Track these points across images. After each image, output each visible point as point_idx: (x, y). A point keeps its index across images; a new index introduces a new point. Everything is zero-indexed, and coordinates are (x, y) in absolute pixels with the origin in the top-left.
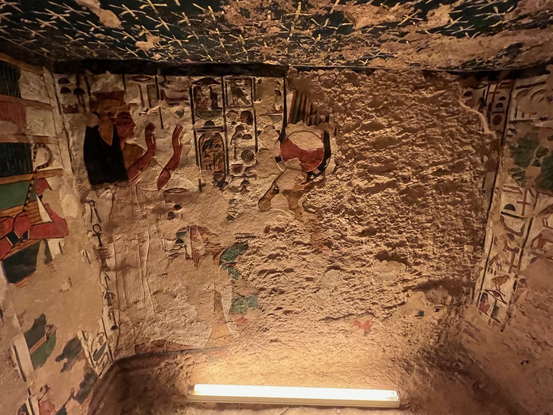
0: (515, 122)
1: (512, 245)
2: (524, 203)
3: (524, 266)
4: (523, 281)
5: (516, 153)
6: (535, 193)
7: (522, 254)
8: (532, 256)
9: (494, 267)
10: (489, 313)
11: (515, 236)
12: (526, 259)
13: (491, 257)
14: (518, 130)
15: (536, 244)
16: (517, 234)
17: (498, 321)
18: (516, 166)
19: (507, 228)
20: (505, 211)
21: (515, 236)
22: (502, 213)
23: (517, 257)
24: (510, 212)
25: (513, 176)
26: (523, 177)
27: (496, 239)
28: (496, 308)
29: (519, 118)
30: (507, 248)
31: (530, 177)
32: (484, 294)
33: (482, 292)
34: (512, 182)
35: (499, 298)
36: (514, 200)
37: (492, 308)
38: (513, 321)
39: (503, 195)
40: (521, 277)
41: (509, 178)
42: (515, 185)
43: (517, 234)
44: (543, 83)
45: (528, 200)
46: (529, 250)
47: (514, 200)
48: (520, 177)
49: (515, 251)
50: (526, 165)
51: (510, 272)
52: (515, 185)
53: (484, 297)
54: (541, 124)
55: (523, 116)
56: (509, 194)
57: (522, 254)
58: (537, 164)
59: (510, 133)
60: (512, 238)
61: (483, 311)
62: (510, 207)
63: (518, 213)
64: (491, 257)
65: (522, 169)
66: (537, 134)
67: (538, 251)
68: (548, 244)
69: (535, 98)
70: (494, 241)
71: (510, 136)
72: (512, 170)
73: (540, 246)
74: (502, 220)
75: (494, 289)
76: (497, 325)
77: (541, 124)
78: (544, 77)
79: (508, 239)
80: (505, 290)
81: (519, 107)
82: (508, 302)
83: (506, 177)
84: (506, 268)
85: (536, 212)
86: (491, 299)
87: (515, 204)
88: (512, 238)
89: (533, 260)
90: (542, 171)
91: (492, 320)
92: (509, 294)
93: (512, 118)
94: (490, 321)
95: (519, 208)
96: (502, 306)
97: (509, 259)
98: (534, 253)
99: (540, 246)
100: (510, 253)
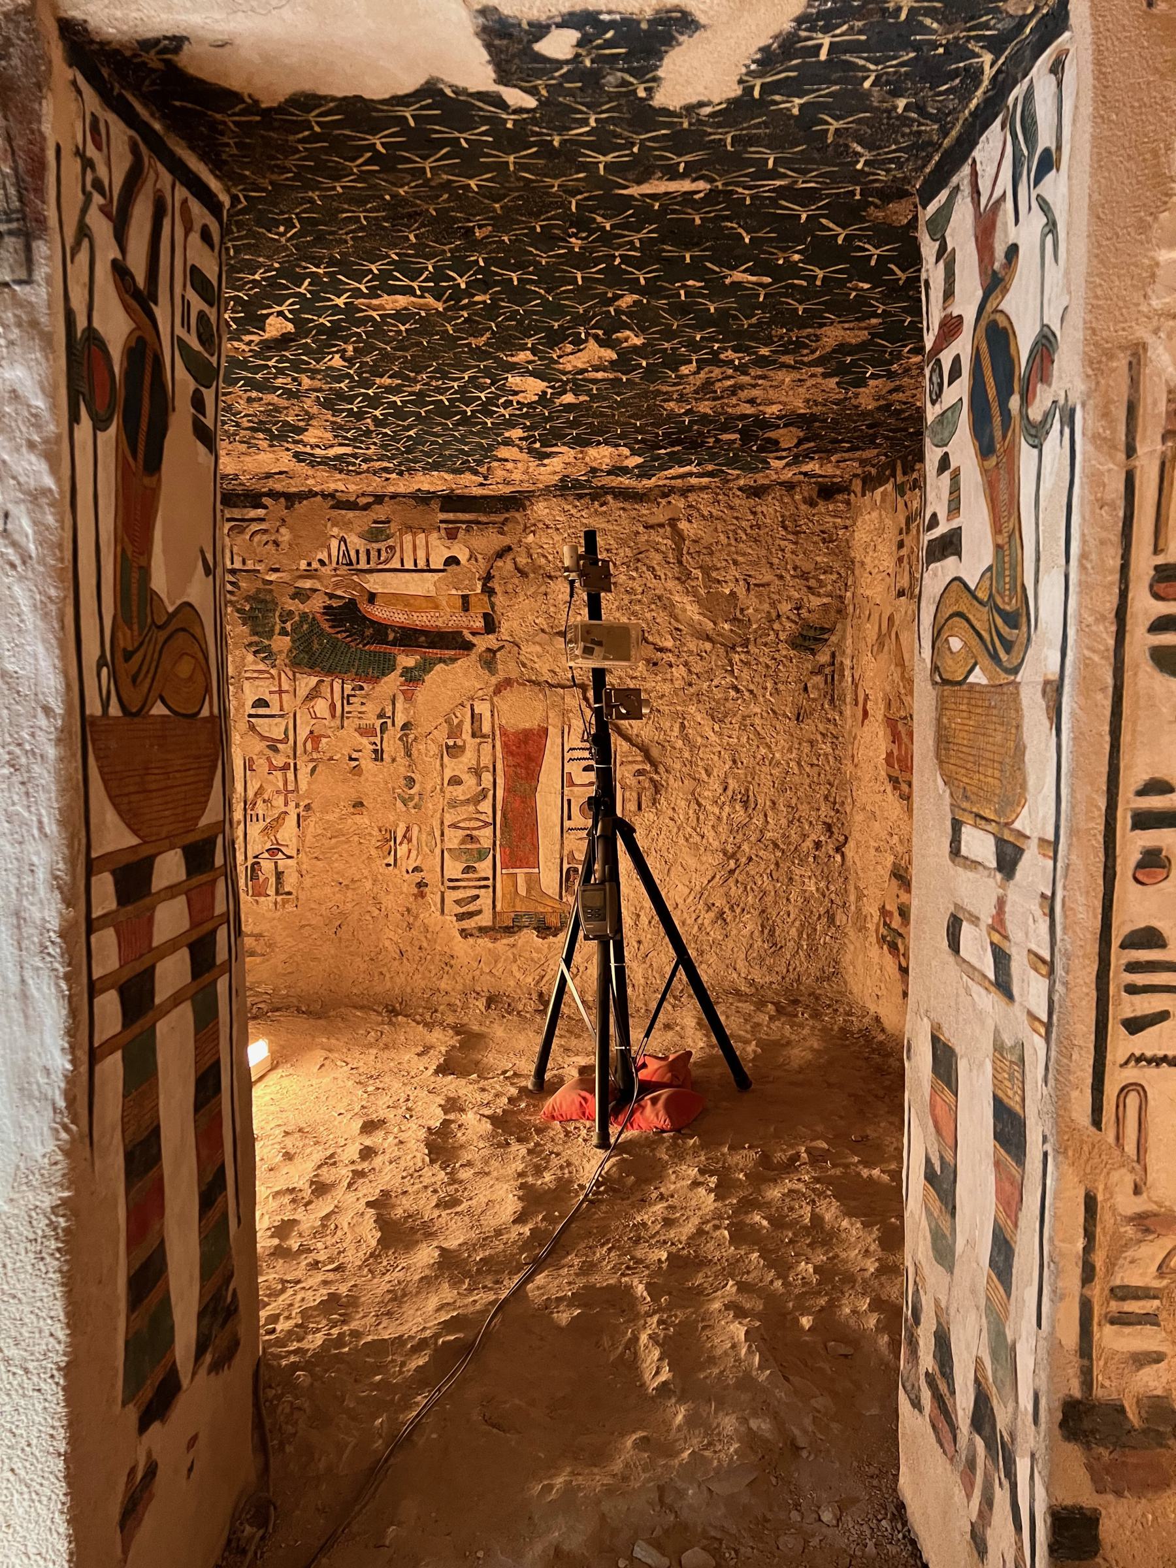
0: (233, 572)
1: (279, 761)
2: (281, 692)
3: (303, 786)
4: (308, 807)
5: (247, 618)
6: (290, 674)
7: (295, 769)
8: (311, 765)
9: (260, 808)
10: (271, 891)
11: (279, 746)
12: (304, 770)
13: (250, 795)
14: (243, 585)
15: (309, 745)
16: (280, 741)
17: (289, 893)
18: (256, 638)
19: (264, 738)
20: (253, 712)
21: (279, 746)
22: (250, 716)
23: (290, 775)
24: (261, 711)
25: (255, 653)
26: (271, 654)
27: (251, 759)
28: (279, 875)
29: (238, 565)
30: (272, 768)
31: (280, 652)
32: (253, 865)
33: (249, 864)
34: (255, 662)
35: (280, 855)
36: (264, 689)
37: (273, 880)
38: (308, 882)
39: (247, 685)
40: (302, 804)
41: (250, 658)
42: (262, 667)
43: (280, 741)
44: (263, 520)
45: (285, 687)
46: (305, 758)
47: (264, 689)
48: (265, 652)
49: (286, 767)
50: (270, 634)
51: (286, 804)
52: (262, 667)
53: (255, 868)
54: (273, 577)
55: (244, 563)
56: (257, 682)
57: (295, 769)
58: (283, 632)
59: (229, 587)
60: (276, 750)
61: (260, 895)
62: (261, 703)
63: (275, 710)
64: (250, 795)
65: (266, 642)
66: (271, 591)
67: (315, 756)
68: (324, 740)
69: (256, 539)
70: (249, 765)
71: (230, 592)
72: (250, 645)
73: (316, 749)
74: (252, 728)
75: (268, 846)
76: (288, 901)
77: (273, 577)
78: (261, 512)
79: (271, 753)
80: (286, 836)
81: (235, 549)
82: (294, 853)
83: (243, 658)
84: (279, 801)
85: (299, 701)
86: (267, 866)
87: (267, 697)
88: (276, 750)
89: (313, 770)
90: (293, 641)
91: (279, 898)
92: (294, 840)
93: (229, 566)
94: (276, 903)
95: (274, 700)
96: (287, 867)
97: (281, 785)
98: (312, 760)
99: (316, 749)
100: (279, 774)
